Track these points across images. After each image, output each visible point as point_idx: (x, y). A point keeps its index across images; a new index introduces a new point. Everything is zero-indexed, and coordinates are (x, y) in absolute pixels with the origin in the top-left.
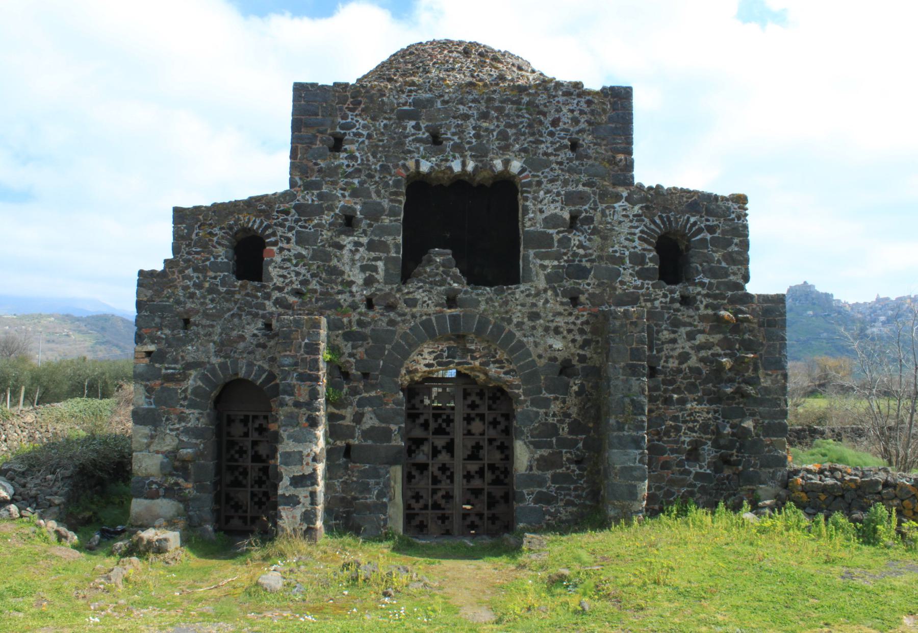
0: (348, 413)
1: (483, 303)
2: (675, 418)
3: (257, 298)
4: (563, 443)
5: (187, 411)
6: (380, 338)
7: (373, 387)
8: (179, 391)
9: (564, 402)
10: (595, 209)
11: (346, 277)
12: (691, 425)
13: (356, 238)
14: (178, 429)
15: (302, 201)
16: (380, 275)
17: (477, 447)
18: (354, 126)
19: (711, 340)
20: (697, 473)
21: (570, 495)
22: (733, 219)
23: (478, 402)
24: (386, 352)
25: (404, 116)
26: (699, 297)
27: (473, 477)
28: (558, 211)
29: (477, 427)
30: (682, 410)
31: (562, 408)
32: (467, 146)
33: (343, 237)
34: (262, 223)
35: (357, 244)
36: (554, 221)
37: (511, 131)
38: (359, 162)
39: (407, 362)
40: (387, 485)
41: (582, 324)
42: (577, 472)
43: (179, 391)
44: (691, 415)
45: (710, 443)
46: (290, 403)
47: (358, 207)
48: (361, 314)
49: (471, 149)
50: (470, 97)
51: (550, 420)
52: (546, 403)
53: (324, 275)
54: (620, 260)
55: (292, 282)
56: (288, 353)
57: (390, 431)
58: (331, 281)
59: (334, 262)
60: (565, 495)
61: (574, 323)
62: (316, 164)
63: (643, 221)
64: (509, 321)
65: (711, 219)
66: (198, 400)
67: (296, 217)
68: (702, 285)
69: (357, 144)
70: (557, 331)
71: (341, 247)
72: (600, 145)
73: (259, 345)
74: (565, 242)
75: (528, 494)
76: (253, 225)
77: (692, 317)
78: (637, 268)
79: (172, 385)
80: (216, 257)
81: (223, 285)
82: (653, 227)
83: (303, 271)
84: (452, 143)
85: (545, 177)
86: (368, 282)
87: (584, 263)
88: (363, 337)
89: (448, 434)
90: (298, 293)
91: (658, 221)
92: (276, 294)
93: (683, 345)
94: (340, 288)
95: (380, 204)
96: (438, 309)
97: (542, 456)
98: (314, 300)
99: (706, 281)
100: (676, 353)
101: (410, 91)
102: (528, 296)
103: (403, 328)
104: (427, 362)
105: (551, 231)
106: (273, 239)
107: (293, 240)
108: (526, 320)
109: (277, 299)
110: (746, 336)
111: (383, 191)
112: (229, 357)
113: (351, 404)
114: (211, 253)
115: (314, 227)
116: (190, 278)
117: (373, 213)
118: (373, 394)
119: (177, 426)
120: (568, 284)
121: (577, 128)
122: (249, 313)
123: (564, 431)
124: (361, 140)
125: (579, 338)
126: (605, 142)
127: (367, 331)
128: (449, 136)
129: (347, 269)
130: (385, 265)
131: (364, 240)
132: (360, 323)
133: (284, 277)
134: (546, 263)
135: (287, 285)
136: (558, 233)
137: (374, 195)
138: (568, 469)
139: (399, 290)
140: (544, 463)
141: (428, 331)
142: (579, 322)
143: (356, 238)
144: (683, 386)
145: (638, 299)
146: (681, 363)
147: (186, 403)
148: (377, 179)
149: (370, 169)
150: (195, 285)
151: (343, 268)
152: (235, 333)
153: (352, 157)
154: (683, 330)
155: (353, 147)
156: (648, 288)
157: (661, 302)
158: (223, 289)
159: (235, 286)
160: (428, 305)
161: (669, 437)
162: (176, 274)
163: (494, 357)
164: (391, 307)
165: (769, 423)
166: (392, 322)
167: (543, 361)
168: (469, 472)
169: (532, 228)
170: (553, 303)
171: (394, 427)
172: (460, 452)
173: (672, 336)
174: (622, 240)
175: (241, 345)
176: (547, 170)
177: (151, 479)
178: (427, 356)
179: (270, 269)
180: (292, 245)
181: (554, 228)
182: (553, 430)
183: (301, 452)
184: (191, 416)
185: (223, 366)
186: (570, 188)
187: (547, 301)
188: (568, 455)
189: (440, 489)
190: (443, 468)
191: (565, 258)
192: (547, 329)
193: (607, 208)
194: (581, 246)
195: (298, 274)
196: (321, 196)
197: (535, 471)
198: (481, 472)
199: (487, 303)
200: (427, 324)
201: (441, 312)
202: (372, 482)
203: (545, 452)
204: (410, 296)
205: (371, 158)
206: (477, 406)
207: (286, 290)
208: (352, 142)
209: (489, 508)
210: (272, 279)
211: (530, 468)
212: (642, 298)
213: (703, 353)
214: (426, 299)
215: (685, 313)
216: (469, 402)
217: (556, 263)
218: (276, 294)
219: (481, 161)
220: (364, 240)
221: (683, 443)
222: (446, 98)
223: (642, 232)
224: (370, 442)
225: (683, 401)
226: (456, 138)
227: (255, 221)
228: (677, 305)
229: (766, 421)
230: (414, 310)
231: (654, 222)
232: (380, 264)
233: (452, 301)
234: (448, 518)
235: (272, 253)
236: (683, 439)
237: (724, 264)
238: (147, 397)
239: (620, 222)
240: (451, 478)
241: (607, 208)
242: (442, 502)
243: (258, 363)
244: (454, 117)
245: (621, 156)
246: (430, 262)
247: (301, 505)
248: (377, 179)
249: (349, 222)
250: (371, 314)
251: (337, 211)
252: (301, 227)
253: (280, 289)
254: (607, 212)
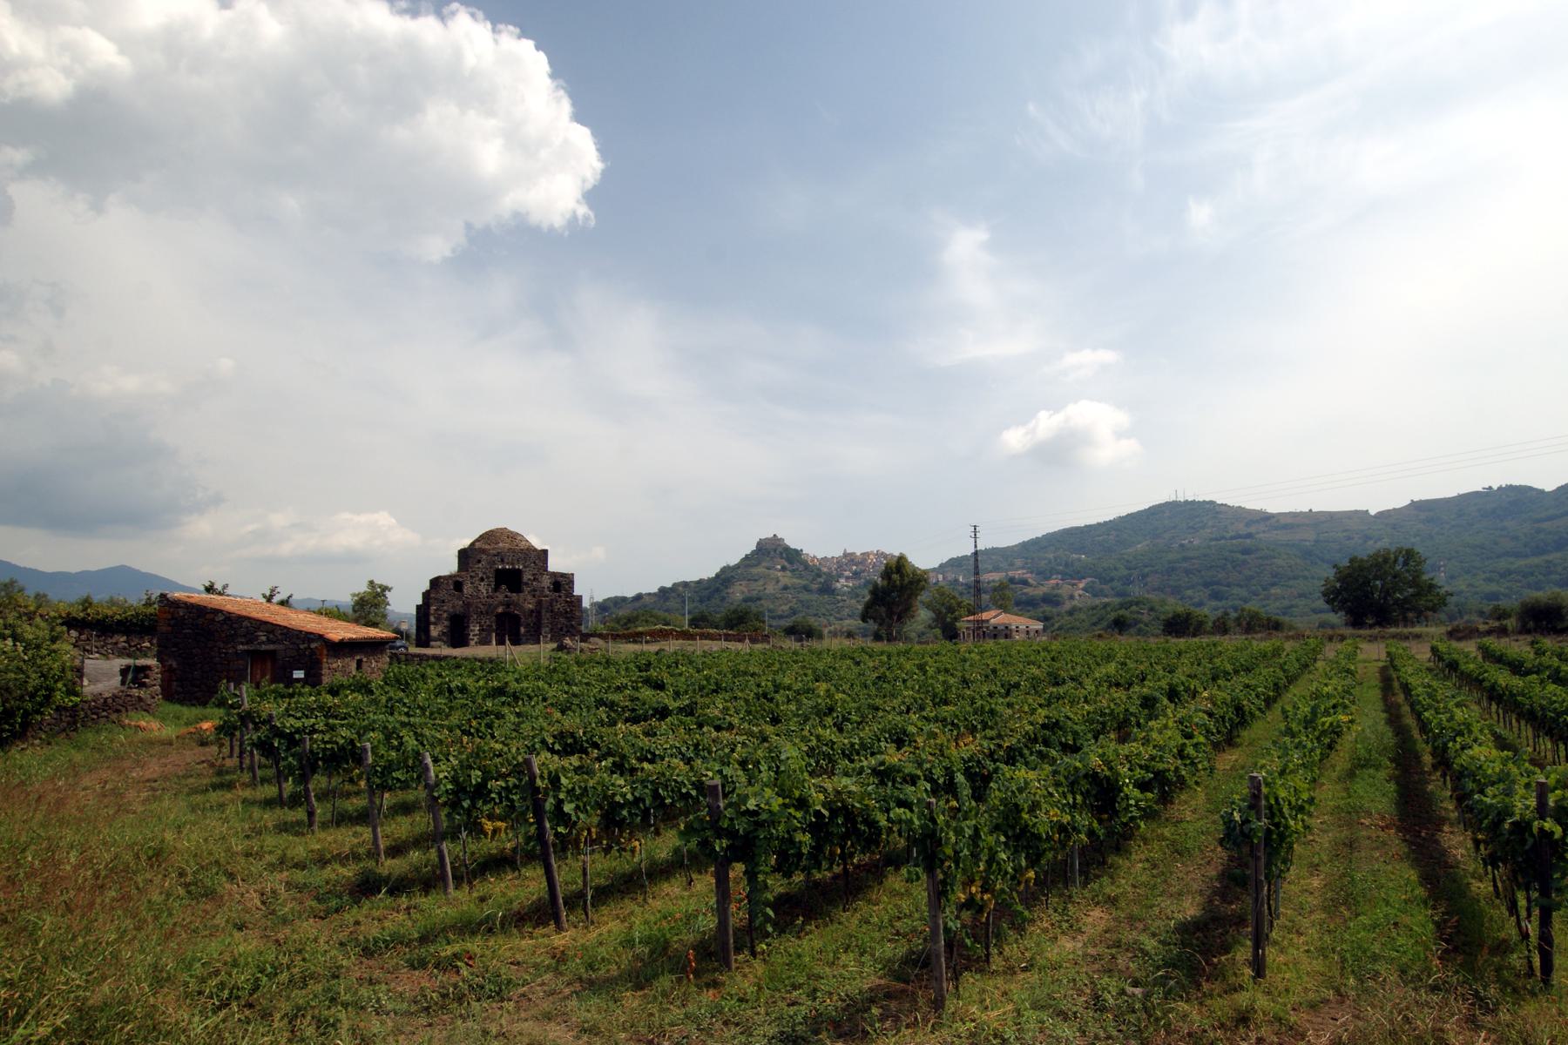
6: (491, 605)
117: (488, 578)
140: (528, 632)
141: (501, 604)
170: (529, 597)
249: (482, 579)
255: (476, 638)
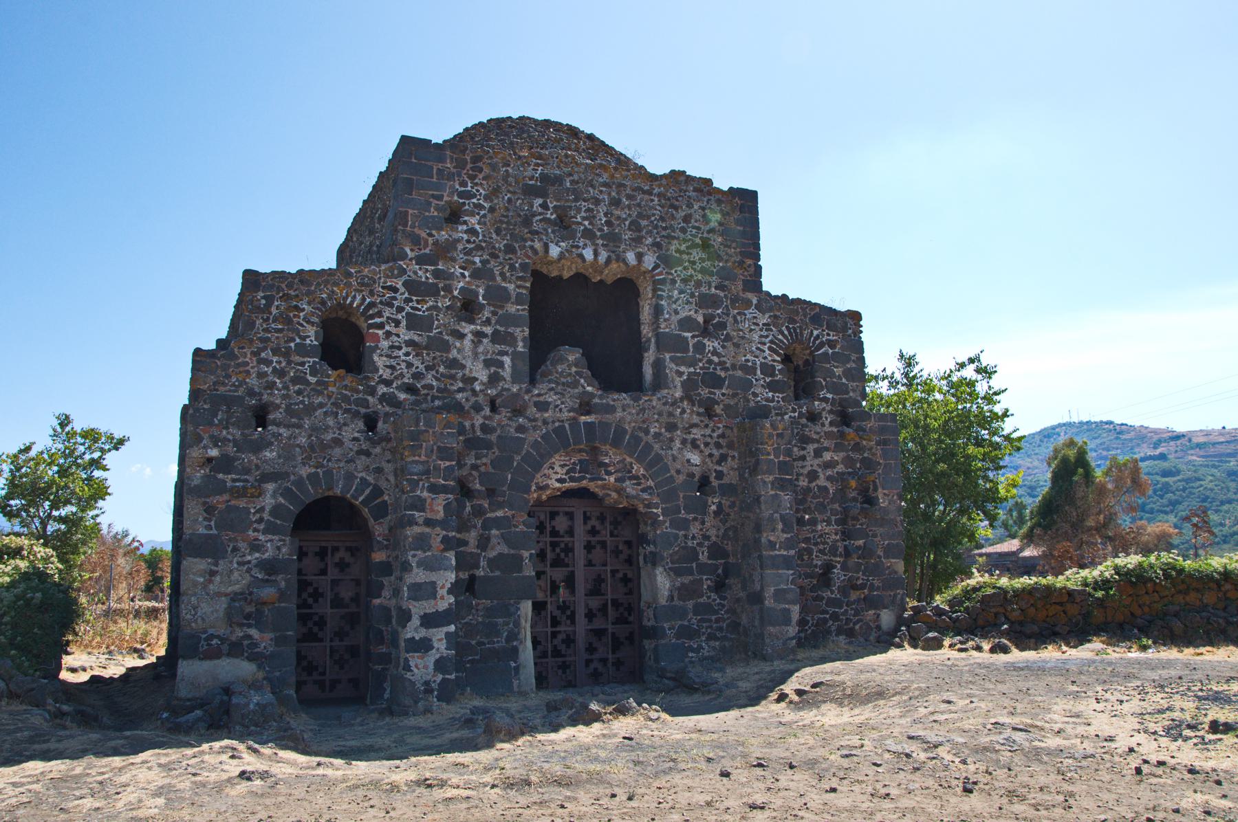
0: (472, 537)
1: (619, 410)
2: (807, 540)
3: (358, 391)
4: (702, 568)
5: (262, 537)
7: (500, 506)
8: (252, 511)
9: (703, 523)
10: (728, 315)
11: (467, 372)
12: (821, 547)
13: (479, 327)
14: (249, 562)
15: (414, 277)
16: (507, 372)
17: (599, 580)
18: (475, 196)
19: (836, 458)
20: (829, 598)
21: (711, 627)
22: (850, 336)
23: (598, 527)
24: (515, 464)
25: (531, 192)
26: (824, 414)
27: (595, 615)
28: (692, 313)
29: (597, 554)
30: (813, 531)
31: (701, 530)
32: (598, 234)
33: (464, 324)
34: (364, 299)
35: (479, 335)
36: (687, 323)
37: (644, 223)
38: (480, 238)
39: (538, 476)
40: (517, 624)
41: (719, 437)
42: (718, 601)
43: (252, 511)
44: (821, 536)
45: (839, 566)
46: (421, 521)
47: (481, 291)
48: (485, 418)
49: (602, 237)
50: (601, 180)
51: (690, 544)
52: (684, 525)
53: (442, 369)
54: (752, 371)
55: (402, 376)
56: (417, 458)
57: (521, 558)
58: (453, 377)
59: (454, 353)
60: (707, 628)
61: (710, 436)
62: (430, 235)
63: (772, 330)
64: (647, 432)
65: (831, 333)
66: (278, 522)
67: (406, 295)
68: (825, 400)
69: (478, 217)
70: (694, 444)
71: (461, 336)
72: (730, 247)
73: (360, 452)
74: (700, 348)
75: (669, 629)
76: (352, 302)
77: (818, 433)
78: (768, 380)
79: (242, 503)
80: (304, 338)
81: (313, 374)
82: (780, 337)
83: (417, 363)
84: (582, 228)
85: (678, 276)
86: (494, 379)
87: (718, 372)
88: (489, 445)
89: (567, 565)
90: (410, 389)
91: (786, 332)
92: (382, 389)
93: (811, 463)
94: (461, 385)
95: (506, 289)
96: (572, 414)
97: (682, 584)
98: (429, 398)
99: (829, 396)
100: (805, 471)
101: (538, 165)
102: (665, 404)
103: (535, 436)
104: (559, 476)
105: (686, 334)
106: (378, 320)
107: (404, 323)
108: (663, 430)
109: (384, 394)
110: (866, 455)
111: (508, 274)
112: (322, 466)
113: (475, 527)
114: (298, 332)
115: (428, 309)
116: (268, 362)
117: (498, 296)
118: (500, 514)
119: (249, 558)
120: (704, 392)
121: (707, 228)
122: (347, 411)
123: (703, 557)
124: (482, 212)
125: (715, 452)
126: (734, 245)
127: (493, 437)
128: (579, 220)
129: (469, 364)
130: (512, 360)
131: (488, 330)
132: (485, 428)
133: (392, 367)
134: (683, 369)
135: (396, 378)
136: (693, 337)
137: (499, 278)
138: (709, 597)
139: (528, 391)
140: (685, 592)
141: (559, 439)
142: (715, 435)
143: (479, 327)
144: (812, 506)
145: (771, 412)
146: (810, 482)
147: (262, 527)
148: (501, 259)
149: (494, 247)
150: (275, 370)
151: (464, 362)
152: (329, 436)
153: (472, 231)
154: (811, 447)
155: (473, 221)
156: (778, 402)
157: (790, 417)
158: (313, 380)
159: (328, 376)
160: (561, 410)
161: (803, 560)
162: (249, 356)
163: (630, 472)
164: (518, 412)
165: (888, 544)
166: (521, 429)
167: (682, 478)
168: (590, 610)
169: (667, 330)
170: (690, 414)
171: (526, 554)
172: (581, 586)
173: (802, 453)
174: (754, 349)
175: (337, 452)
176: (680, 268)
177: (211, 631)
178: (557, 469)
179: (376, 358)
180: (402, 330)
181: (689, 332)
182: (692, 555)
183: (434, 583)
184: (269, 545)
185: (313, 478)
186: (704, 289)
187: (683, 411)
188: (709, 582)
189: (560, 632)
190: (563, 608)
191: (701, 365)
192: (684, 442)
193: (739, 314)
194: (715, 353)
195: (409, 365)
196: (437, 274)
197: (676, 602)
198: (604, 609)
199: (624, 410)
200: (559, 431)
201: (574, 419)
202: (500, 620)
203: (686, 579)
204: (541, 399)
205: (494, 236)
206: (598, 532)
207: (394, 385)
208: (472, 214)
209: (613, 652)
210: (377, 370)
211: (671, 598)
212: (773, 412)
213: (829, 472)
214: (559, 402)
215: (813, 431)
216: (589, 527)
217: (692, 370)
218: (382, 389)
219: (613, 252)
220: (488, 330)
221: (816, 566)
222: (576, 177)
223: (771, 342)
224: (497, 573)
225: (813, 522)
226: (586, 223)
227: (354, 297)
228: (804, 421)
229: (886, 542)
230: (546, 415)
231: (782, 333)
232: (507, 360)
233: (586, 407)
234: (568, 667)
235: (376, 338)
236: (815, 562)
237: (844, 380)
238: (205, 519)
239: (751, 330)
240: (572, 618)
241: (739, 314)
242: (563, 647)
243: (360, 475)
244: (585, 201)
245: (749, 262)
246: (562, 360)
247: (434, 651)
248: (501, 259)
249: (468, 308)
250: (497, 417)
251: (456, 293)
252: (412, 308)
253: (387, 383)
254: (739, 318)
255: (439, 636)
